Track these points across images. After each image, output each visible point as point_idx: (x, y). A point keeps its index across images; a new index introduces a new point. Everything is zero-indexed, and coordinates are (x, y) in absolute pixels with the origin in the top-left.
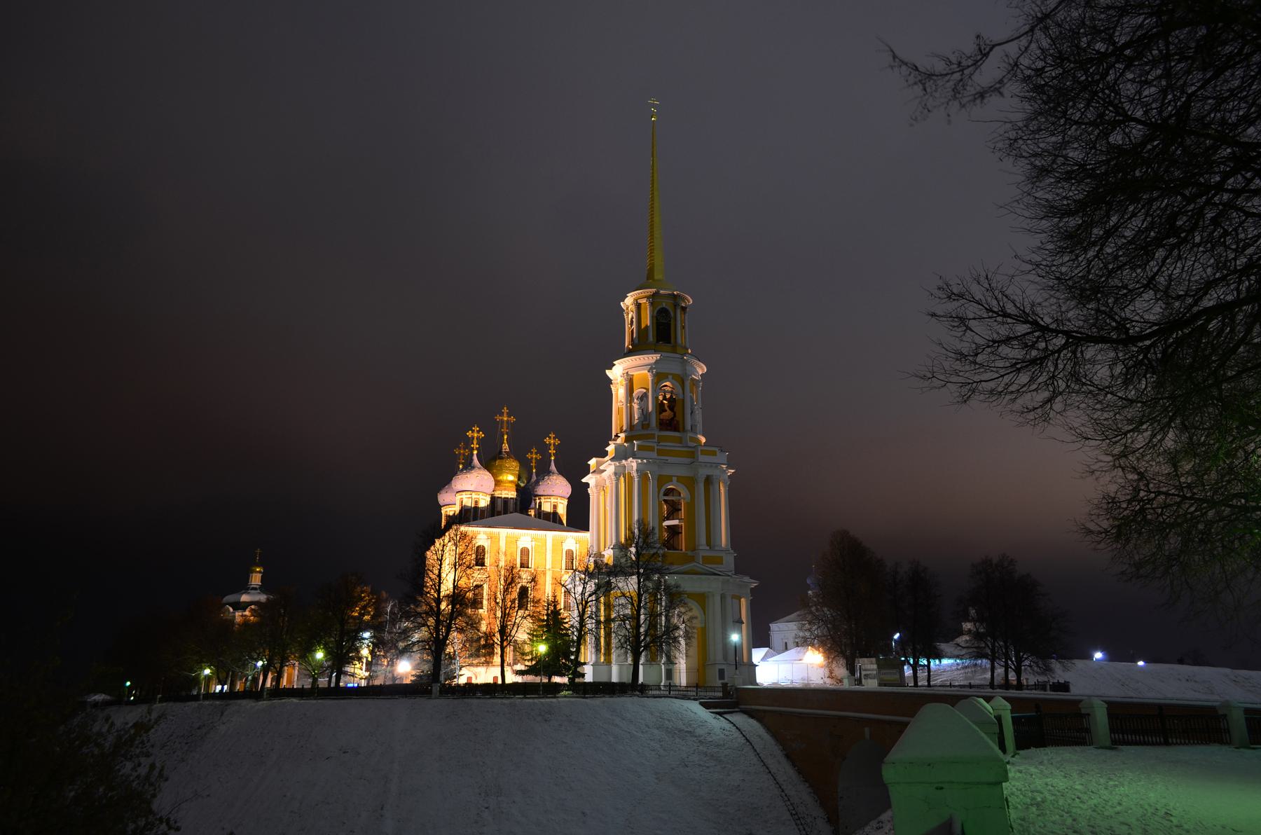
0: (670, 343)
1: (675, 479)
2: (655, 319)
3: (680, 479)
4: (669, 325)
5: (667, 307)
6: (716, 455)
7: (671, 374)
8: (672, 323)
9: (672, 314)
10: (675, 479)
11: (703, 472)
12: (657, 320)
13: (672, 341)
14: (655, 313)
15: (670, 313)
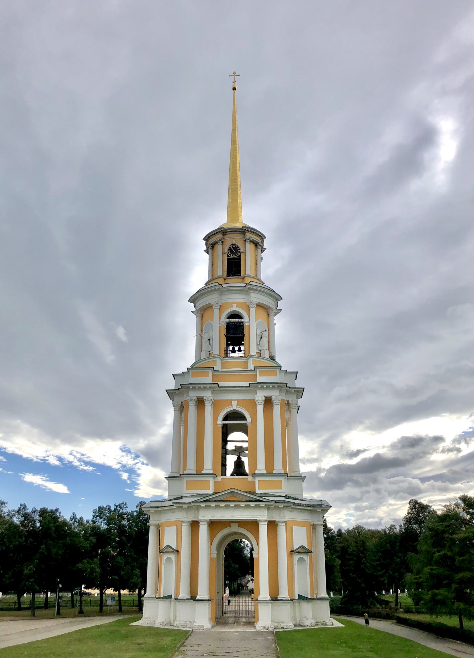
0: (240, 276)
1: (234, 403)
2: (226, 255)
3: (239, 402)
4: (239, 259)
5: (236, 244)
6: (276, 376)
7: (235, 303)
8: (242, 257)
9: (242, 250)
10: (234, 403)
11: (261, 395)
12: (228, 256)
13: (242, 273)
14: (226, 250)
15: (239, 249)
